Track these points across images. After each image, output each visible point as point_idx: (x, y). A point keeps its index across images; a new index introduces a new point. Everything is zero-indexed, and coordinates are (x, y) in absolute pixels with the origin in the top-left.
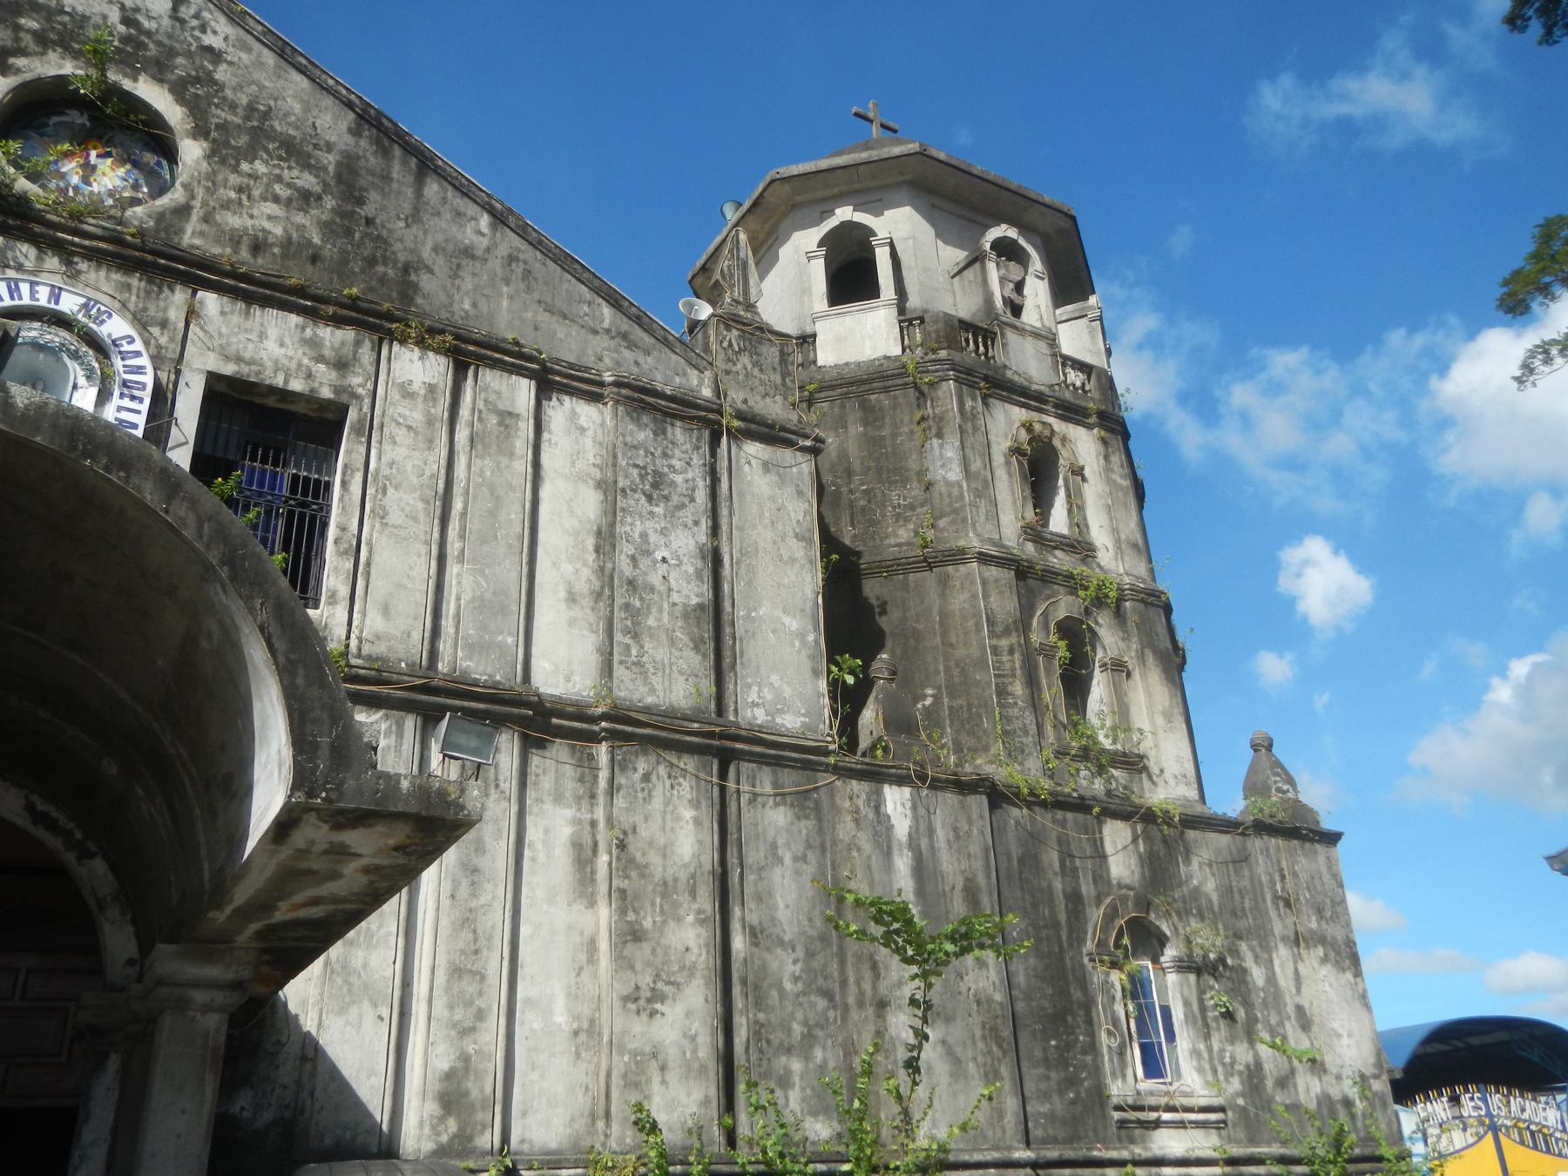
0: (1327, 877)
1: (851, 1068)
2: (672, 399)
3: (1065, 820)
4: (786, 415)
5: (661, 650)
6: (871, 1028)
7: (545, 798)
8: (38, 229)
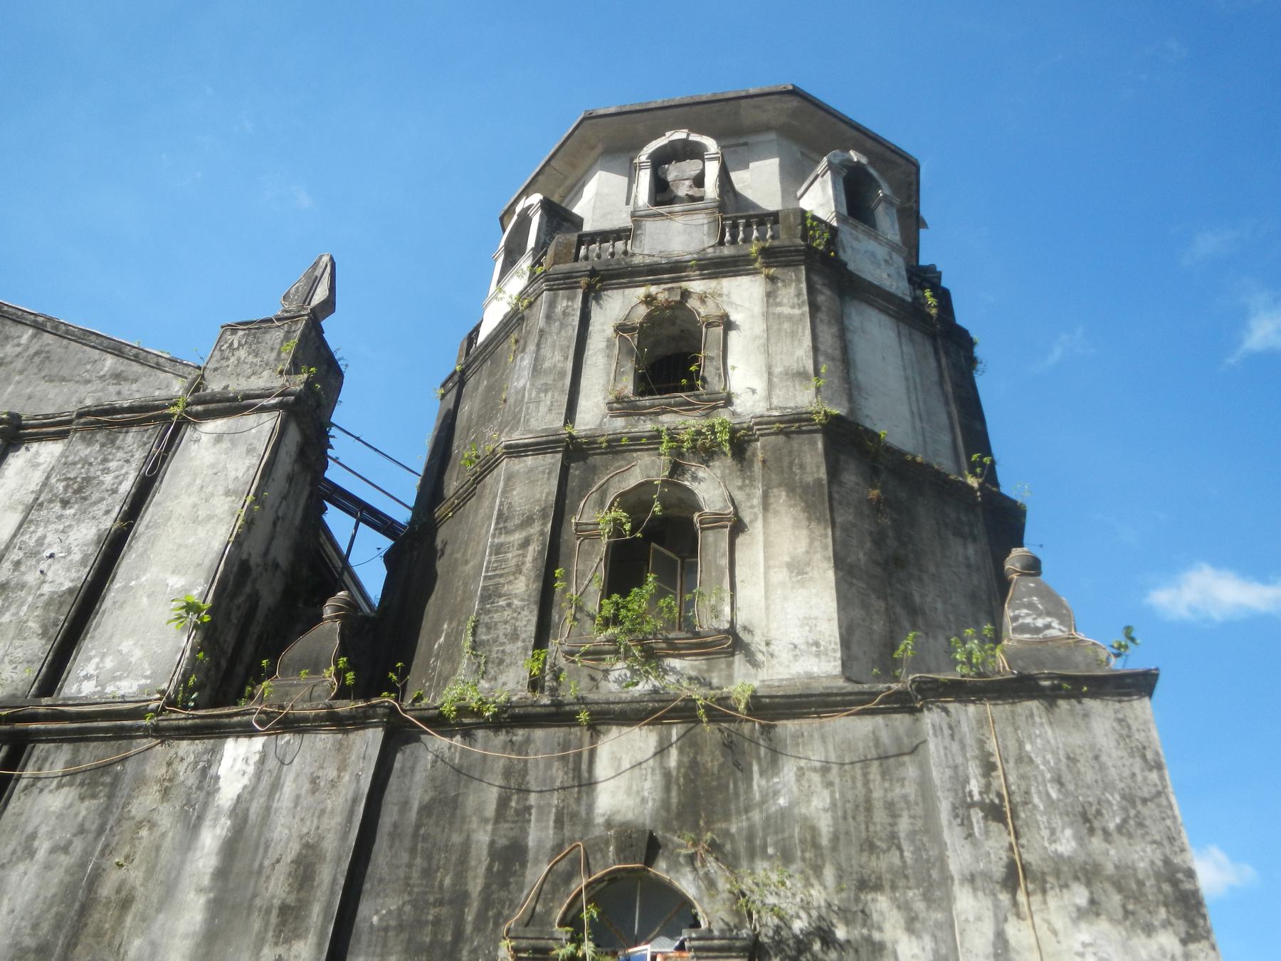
0: (1113, 754)
2: (131, 409)
3: (528, 741)
4: (269, 385)
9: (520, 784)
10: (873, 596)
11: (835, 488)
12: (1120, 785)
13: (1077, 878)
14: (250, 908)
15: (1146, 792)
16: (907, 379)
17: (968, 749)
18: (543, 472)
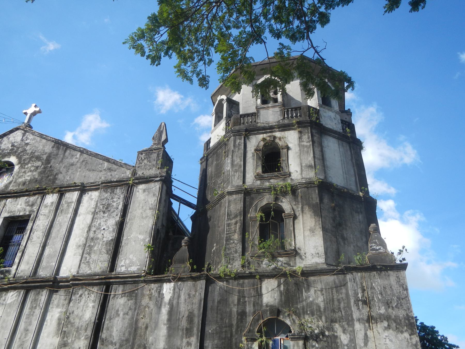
2: (117, 182)
3: (243, 283)
4: (155, 173)
9: (243, 295)
10: (333, 237)
11: (322, 205)
12: (397, 295)
13: (385, 319)
14: (178, 329)
15: (403, 297)
16: (341, 160)
17: (358, 285)
18: (239, 200)
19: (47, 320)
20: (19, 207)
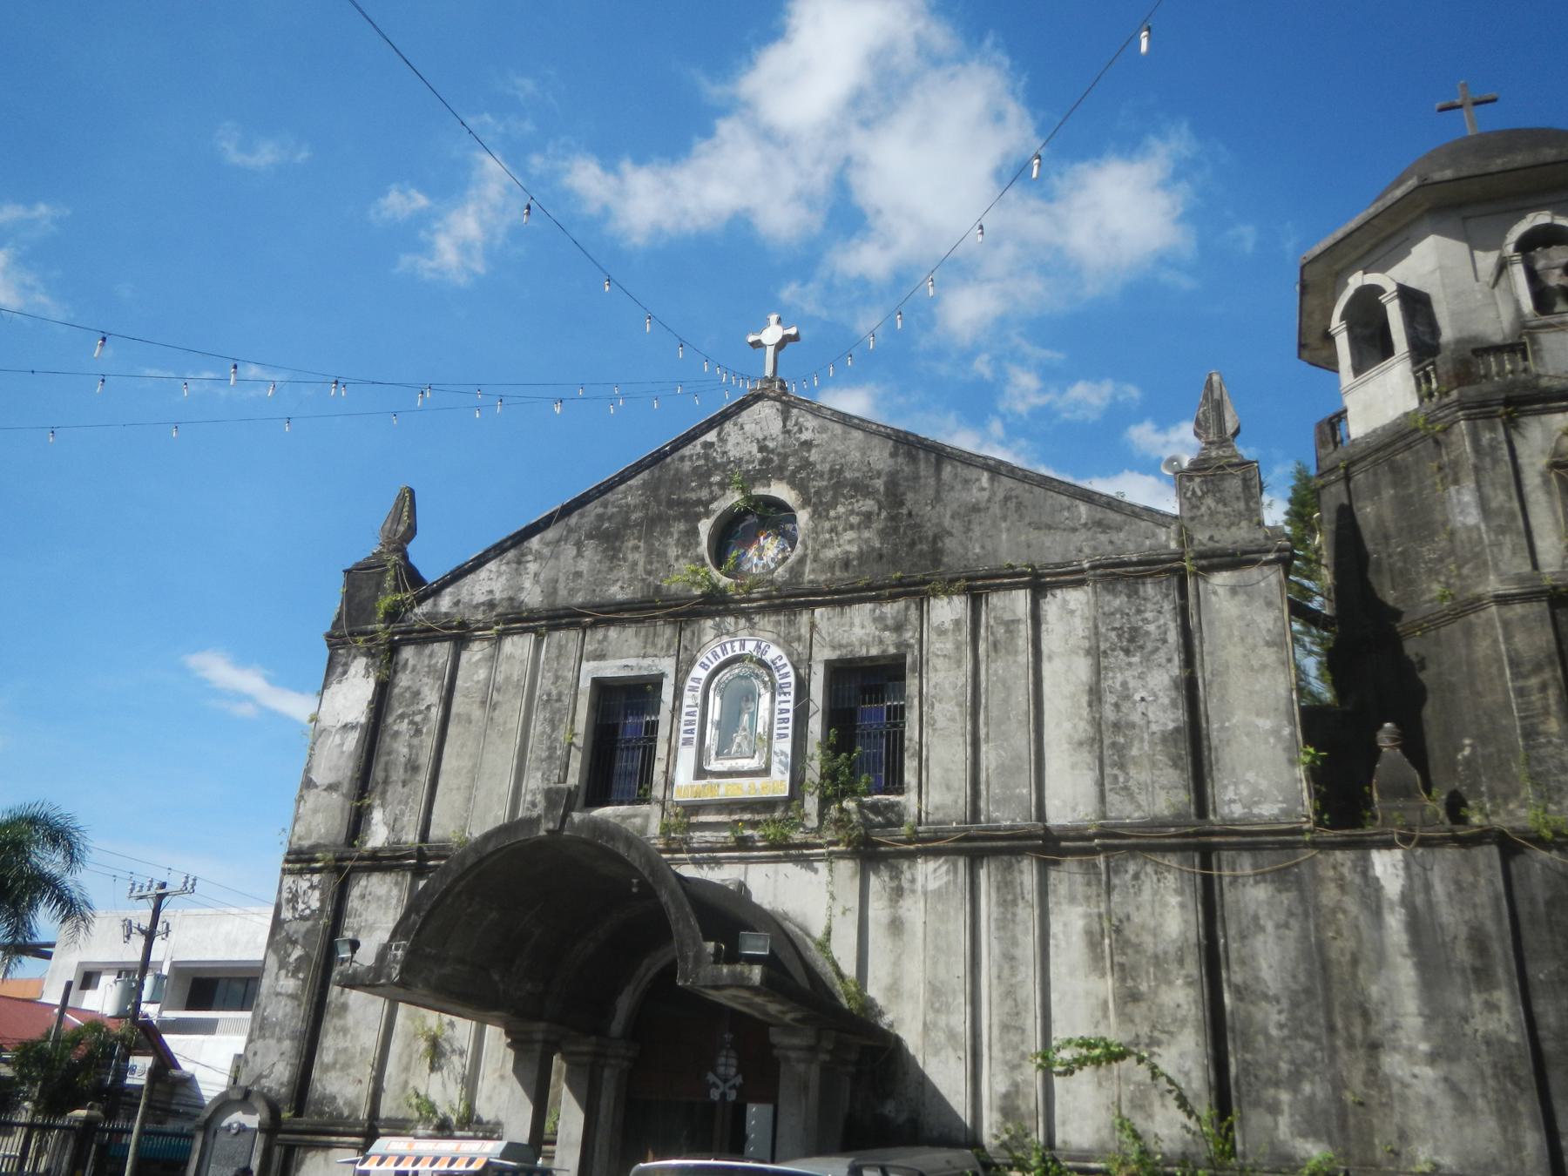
1: (1340, 1101)
2: (1139, 563)
4: (1252, 536)
5: (1144, 774)
6: (1363, 1066)
7: (1062, 900)
8: (732, 606)
19: (1055, 935)
20: (858, 632)
